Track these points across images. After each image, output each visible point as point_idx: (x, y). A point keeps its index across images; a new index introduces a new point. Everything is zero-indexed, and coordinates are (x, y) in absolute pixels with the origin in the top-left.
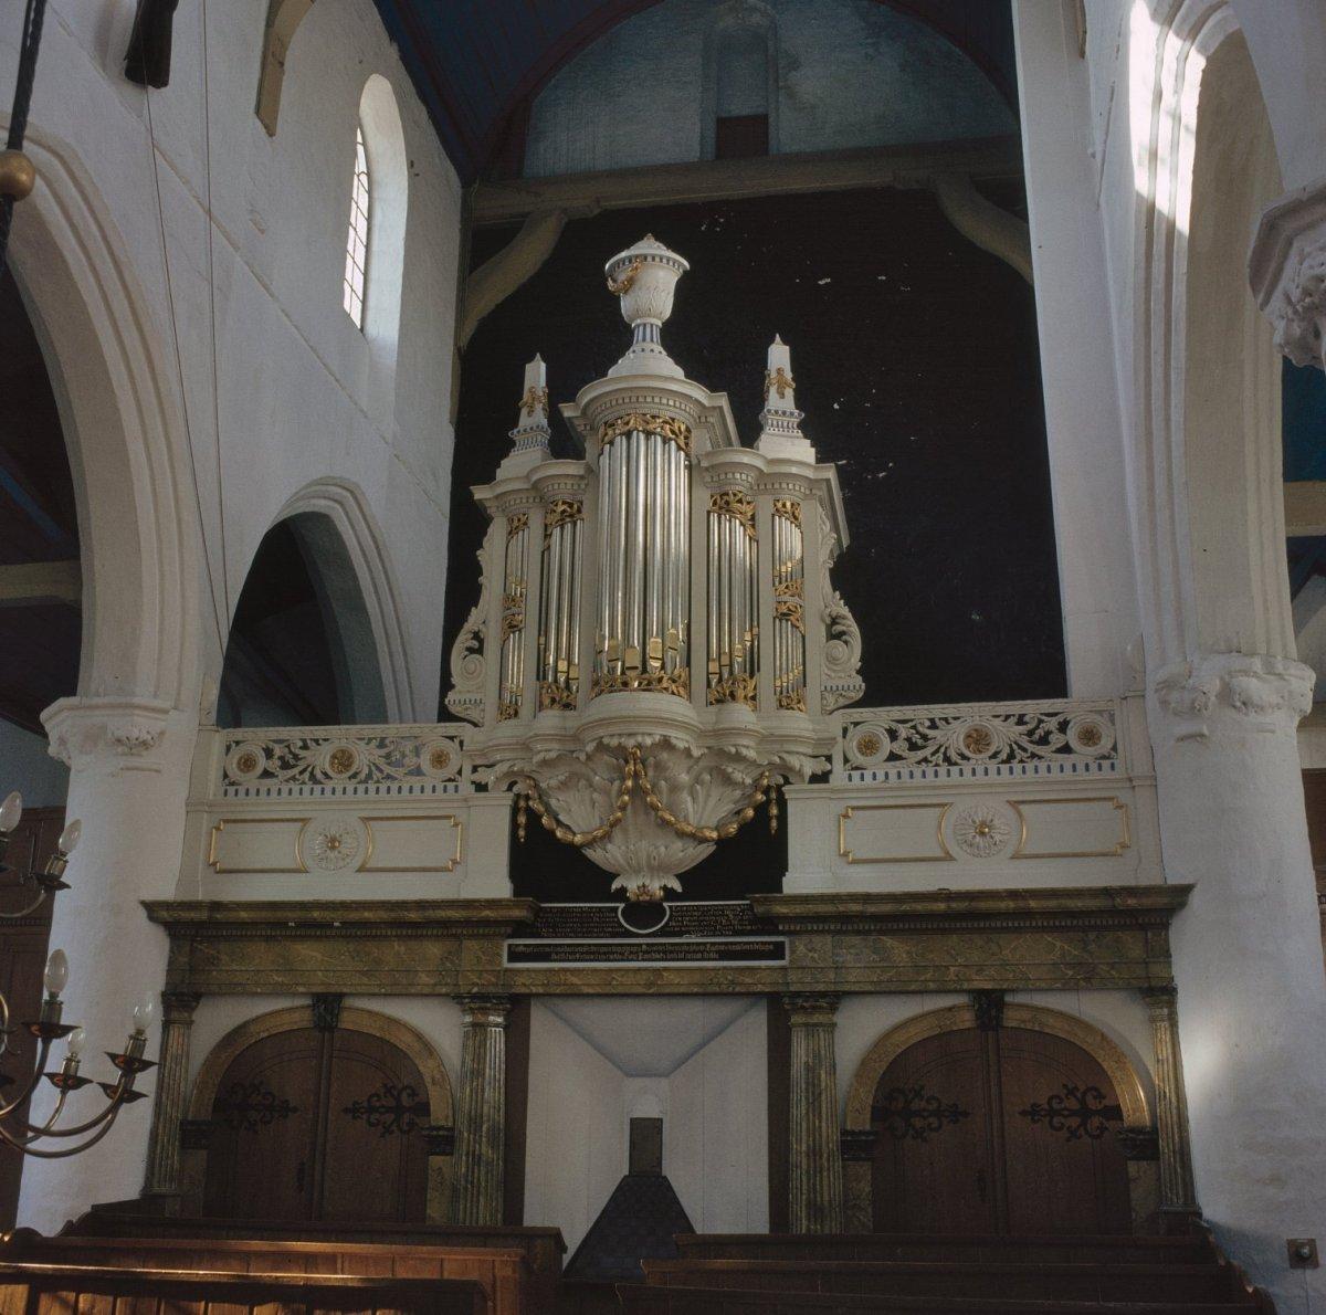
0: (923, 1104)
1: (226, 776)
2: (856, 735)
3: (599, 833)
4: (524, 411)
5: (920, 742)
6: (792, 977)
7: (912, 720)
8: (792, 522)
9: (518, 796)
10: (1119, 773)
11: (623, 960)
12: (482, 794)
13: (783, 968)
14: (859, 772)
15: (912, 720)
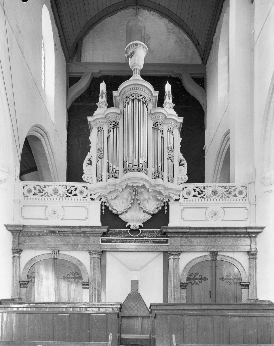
0: (198, 277)
1: (24, 194)
2: (186, 190)
3: (125, 211)
4: (100, 98)
5: (201, 193)
6: (170, 247)
7: (199, 187)
8: (172, 134)
9: (102, 202)
10: (247, 201)
11: (129, 243)
12: (92, 201)
13: (169, 245)
14: (186, 199)
15: (199, 187)
